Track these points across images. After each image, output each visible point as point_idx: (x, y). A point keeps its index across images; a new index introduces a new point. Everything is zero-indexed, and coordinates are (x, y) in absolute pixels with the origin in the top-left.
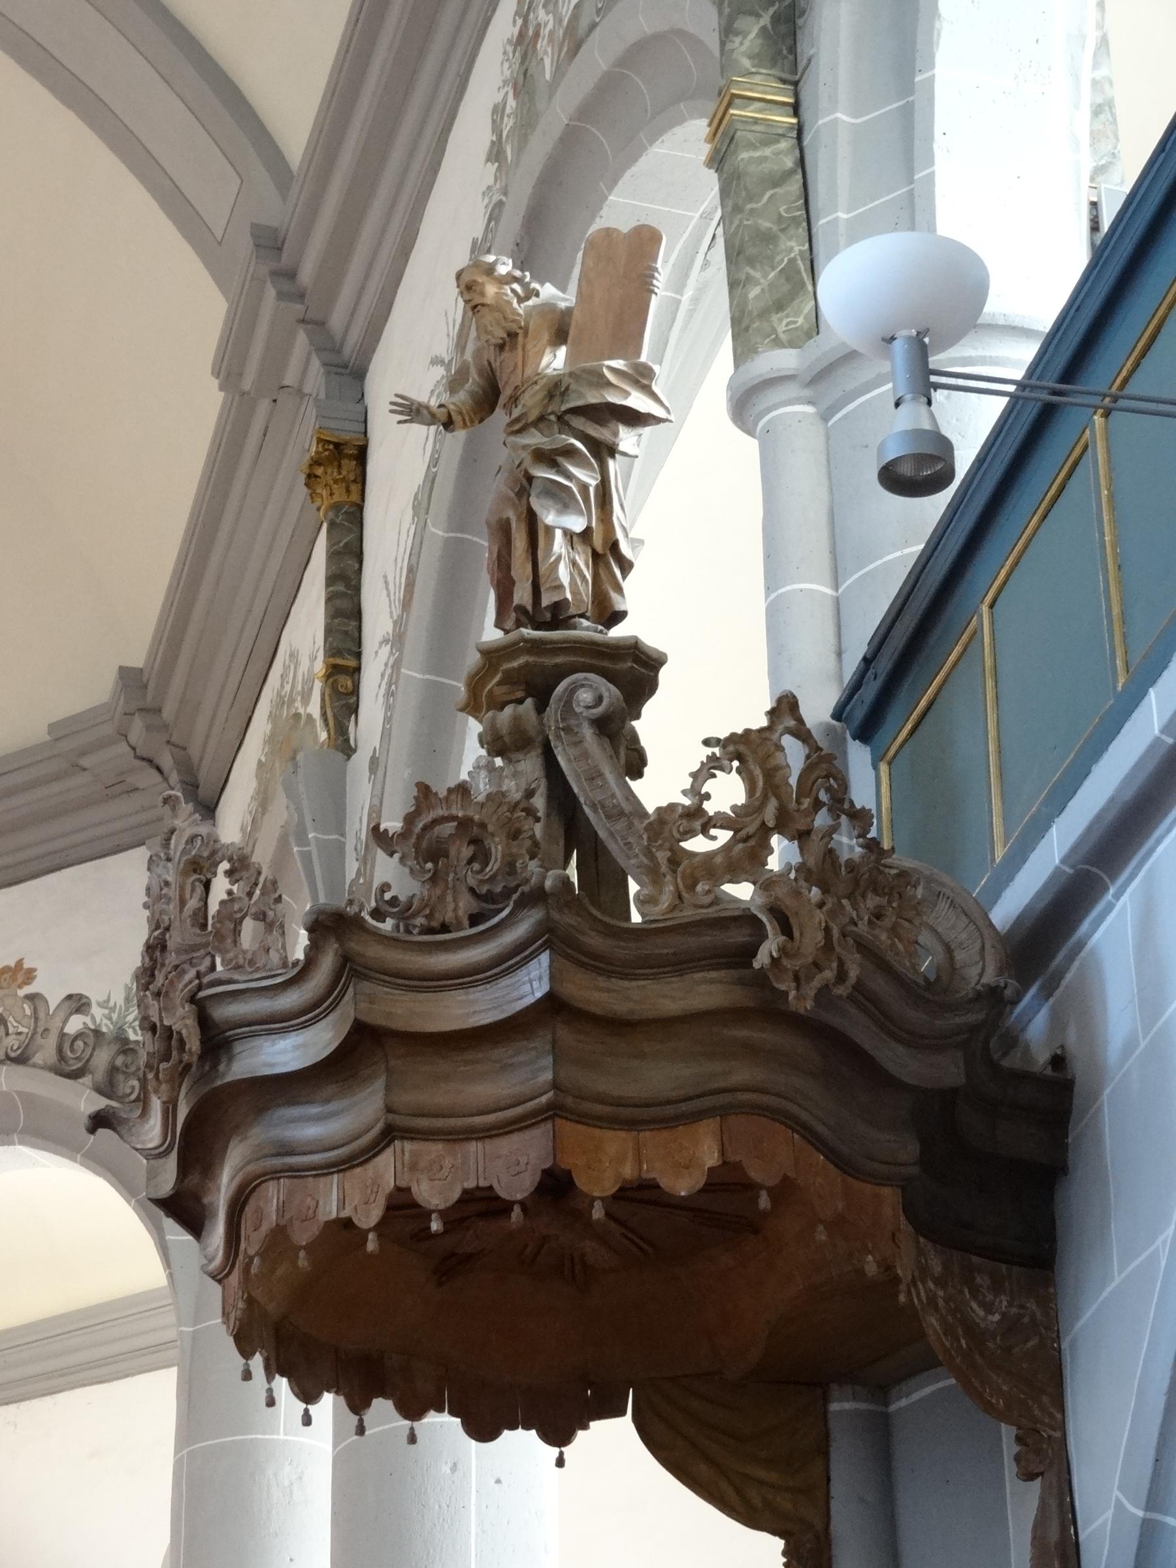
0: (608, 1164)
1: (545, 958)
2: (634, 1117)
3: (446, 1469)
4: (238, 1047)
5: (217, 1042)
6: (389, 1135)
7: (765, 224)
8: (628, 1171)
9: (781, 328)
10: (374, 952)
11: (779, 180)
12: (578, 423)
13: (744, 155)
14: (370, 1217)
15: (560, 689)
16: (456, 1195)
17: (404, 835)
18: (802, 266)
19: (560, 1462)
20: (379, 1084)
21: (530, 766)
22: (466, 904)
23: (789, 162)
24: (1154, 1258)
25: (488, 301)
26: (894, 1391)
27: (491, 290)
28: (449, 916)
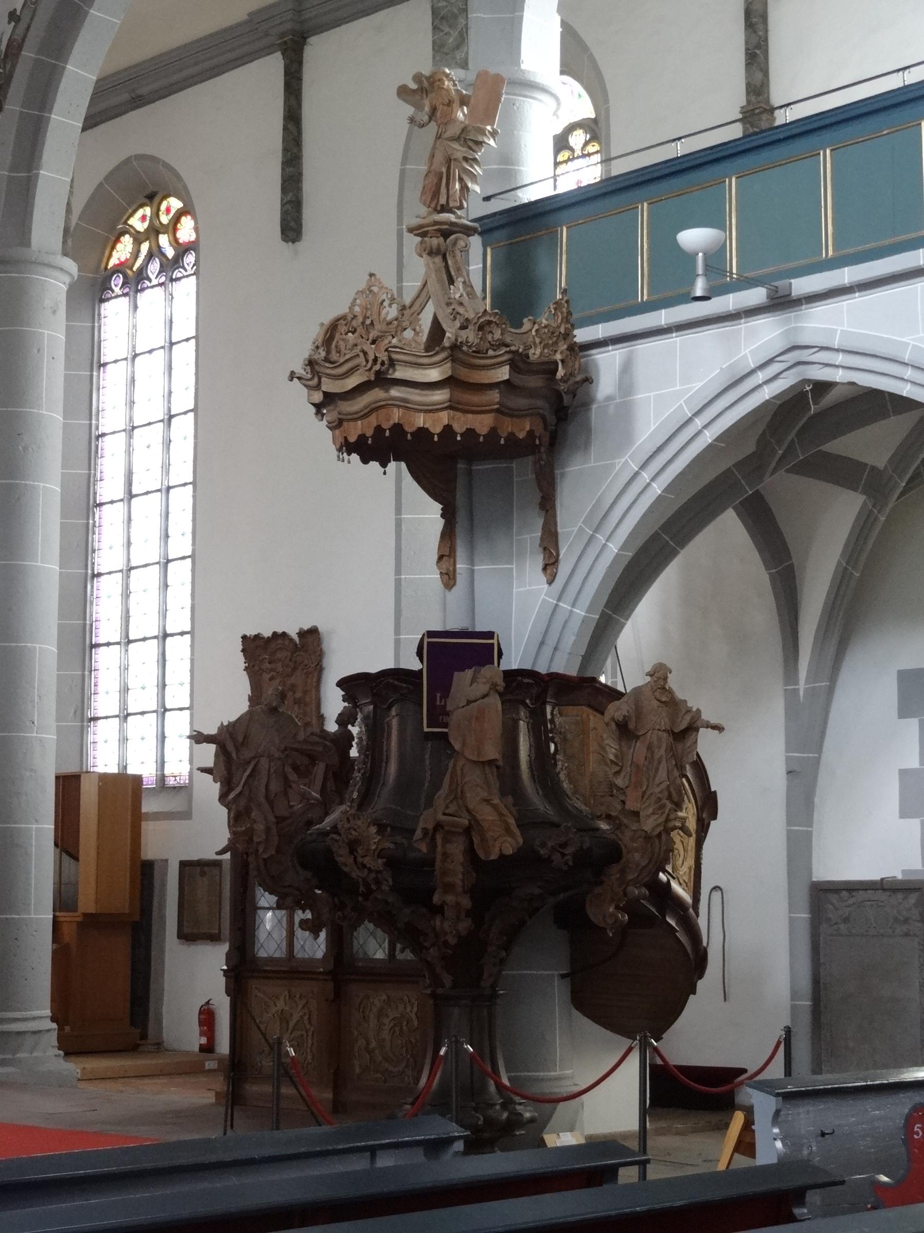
0: (508, 426)
1: (508, 367)
3: (36, 351)
4: (397, 367)
5: (392, 363)
6: (450, 408)
8: (510, 430)
9: (458, 57)
12: (470, 144)
14: (437, 429)
15: (453, 237)
16: (464, 429)
17: (475, 323)
19: (385, 473)
21: (438, 260)
24: (613, 465)
27: (446, 83)
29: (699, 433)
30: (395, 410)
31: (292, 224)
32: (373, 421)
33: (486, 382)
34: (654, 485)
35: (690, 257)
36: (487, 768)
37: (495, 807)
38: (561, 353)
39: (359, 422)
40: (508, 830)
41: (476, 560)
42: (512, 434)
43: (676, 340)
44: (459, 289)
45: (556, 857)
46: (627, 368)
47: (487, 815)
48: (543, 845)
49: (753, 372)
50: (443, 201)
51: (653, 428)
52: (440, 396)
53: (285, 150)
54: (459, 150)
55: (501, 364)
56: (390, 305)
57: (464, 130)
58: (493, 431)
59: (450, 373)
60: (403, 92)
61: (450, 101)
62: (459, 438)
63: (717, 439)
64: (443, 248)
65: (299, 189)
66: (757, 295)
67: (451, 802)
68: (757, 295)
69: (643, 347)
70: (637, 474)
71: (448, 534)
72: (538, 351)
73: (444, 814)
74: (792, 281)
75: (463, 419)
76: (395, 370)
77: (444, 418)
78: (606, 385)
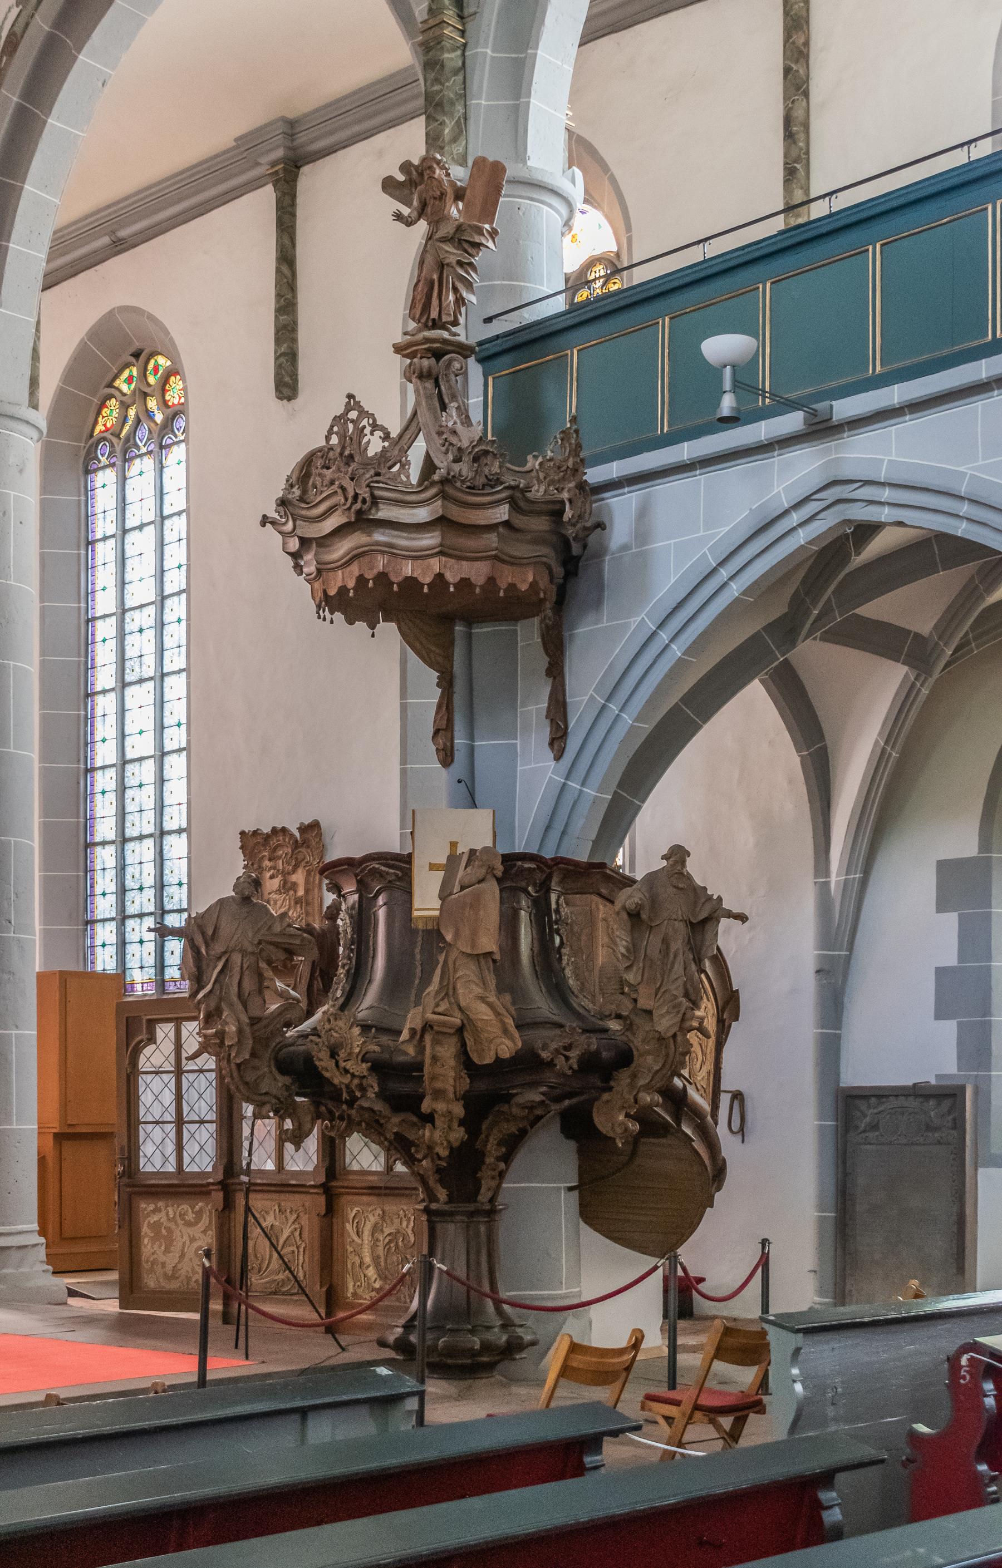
0: (507, 577)
1: (507, 506)
2: (514, 562)
4: (381, 506)
5: (375, 501)
6: (441, 553)
7: (452, 96)
8: (510, 581)
9: (455, 152)
10: (451, 491)
11: (456, 72)
13: (446, 55)
16: (458, 579)
18: (462, 121)
19: (373, 636)
20: (437, 533)
22: (483, 480)
23: (460, 64)
25: (436, 176)
26: (475, 625)
27: (438, 171)
28: (476, 484)
29: (725, 585)
30: (379, 557)
31: (287, 379)
32: (355, 569)
33: (483, 523)
34: (673, 646)
35: (716, 372)
36: (482, 960)
37: (491, 1005)
38: (569, 491)
39: (340, 572)
40: (505, 1031)
41: (477, 733)
42: (512, 587)
43: (701, 479)
44: (452, 417)
45: (560, 1061)
46: (643, 513)
47: (482, 1013)
48: (545, 1047)
49: (786, 513)
50: (434, 314)
51: (673, 581)
52: (430, 540)
53: (279, 296)
54: (452, 254)
55: (498, 503)
56: (372, 434)
57: (459, 228)
58: (491, 580)
59: (440, 512)
60: (389, 185)
61: (442, 194)
62: (452, 589)
63: (744, 593)
64: (434, 372)
65: (294, 340)
66: (793, 421)
67: (443, 999)
68: (793, 421)
69: (663, 490)
70: (654, 634)
71: (446, 705)
72: (542, 489)
73: (434, 1013)
74: (834, 403)
75: (456, 567)
76: (378, 510)
77: (436, 565)
78: (620, 533)
